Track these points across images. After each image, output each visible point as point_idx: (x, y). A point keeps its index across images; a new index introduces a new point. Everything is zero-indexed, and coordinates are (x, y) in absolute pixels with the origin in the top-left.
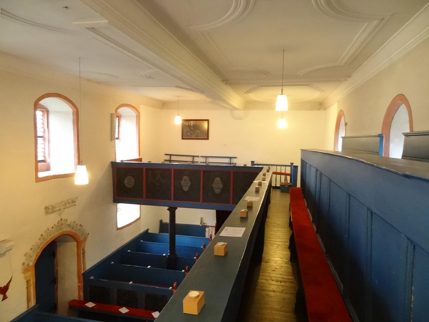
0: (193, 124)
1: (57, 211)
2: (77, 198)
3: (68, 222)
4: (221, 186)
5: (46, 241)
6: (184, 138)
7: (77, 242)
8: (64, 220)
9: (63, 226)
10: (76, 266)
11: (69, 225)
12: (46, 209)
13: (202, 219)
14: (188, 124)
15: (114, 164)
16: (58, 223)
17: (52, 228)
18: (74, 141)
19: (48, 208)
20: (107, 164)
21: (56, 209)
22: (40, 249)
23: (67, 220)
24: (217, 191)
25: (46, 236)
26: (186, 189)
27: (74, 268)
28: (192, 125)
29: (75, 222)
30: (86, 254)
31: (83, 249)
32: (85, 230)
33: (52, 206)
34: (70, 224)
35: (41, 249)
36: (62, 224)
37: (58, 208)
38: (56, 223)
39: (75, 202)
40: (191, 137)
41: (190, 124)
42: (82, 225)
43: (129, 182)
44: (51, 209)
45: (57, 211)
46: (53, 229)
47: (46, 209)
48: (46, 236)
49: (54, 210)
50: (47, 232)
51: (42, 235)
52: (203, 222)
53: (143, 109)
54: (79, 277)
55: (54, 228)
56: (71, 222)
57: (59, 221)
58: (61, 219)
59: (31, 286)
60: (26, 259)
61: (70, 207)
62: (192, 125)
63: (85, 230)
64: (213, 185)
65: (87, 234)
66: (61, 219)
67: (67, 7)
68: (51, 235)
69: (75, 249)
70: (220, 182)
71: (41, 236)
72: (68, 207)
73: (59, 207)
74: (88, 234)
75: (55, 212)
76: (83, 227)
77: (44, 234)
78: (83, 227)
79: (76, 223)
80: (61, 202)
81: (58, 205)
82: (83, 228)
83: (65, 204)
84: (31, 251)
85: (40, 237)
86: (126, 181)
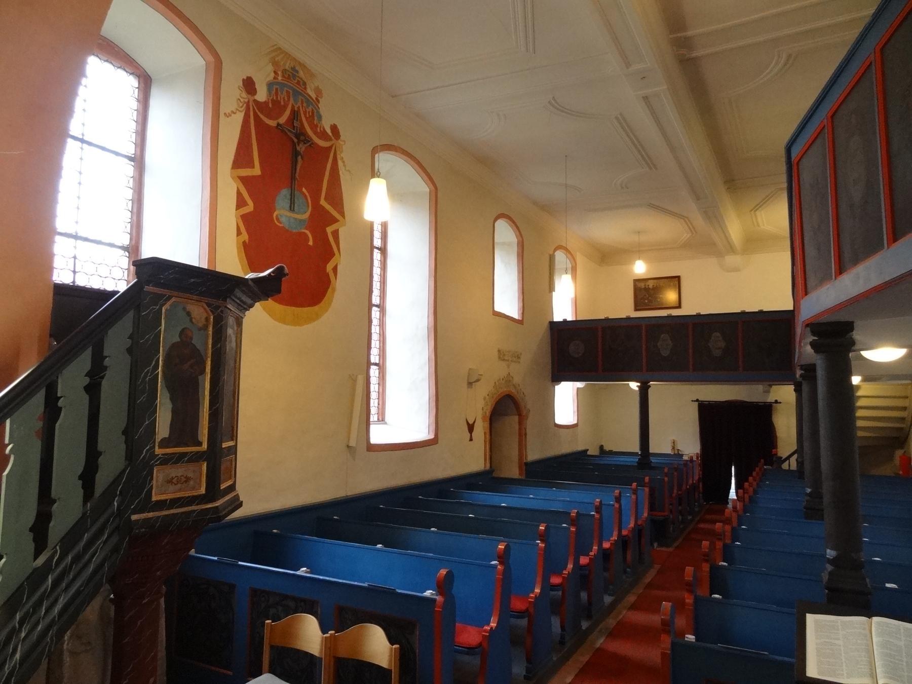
0: (653, 285)
4: (722, 344)
6: (637, 308)
7: (520, 415)
10: (517, 453)
11: (514, 385)
13: (674, 443)
14: (645, 285)
15: (553, 325)
18: (519, 280)
20: (546, 324)
24: (717, 353)
26: (665, 353)
27: (515, 453)
28: (651, 286)
30: (527, 437)
40: (650, 306)
41: (648, 286)
43: (576, 349)
52: (676, 448)
53: (580, 259)
54: (520, 468)
62: (651, 286)
64: (709, 344)
67: (644, 78)
69: (517, 427)
70: (721, 338)
86: (572, 348)
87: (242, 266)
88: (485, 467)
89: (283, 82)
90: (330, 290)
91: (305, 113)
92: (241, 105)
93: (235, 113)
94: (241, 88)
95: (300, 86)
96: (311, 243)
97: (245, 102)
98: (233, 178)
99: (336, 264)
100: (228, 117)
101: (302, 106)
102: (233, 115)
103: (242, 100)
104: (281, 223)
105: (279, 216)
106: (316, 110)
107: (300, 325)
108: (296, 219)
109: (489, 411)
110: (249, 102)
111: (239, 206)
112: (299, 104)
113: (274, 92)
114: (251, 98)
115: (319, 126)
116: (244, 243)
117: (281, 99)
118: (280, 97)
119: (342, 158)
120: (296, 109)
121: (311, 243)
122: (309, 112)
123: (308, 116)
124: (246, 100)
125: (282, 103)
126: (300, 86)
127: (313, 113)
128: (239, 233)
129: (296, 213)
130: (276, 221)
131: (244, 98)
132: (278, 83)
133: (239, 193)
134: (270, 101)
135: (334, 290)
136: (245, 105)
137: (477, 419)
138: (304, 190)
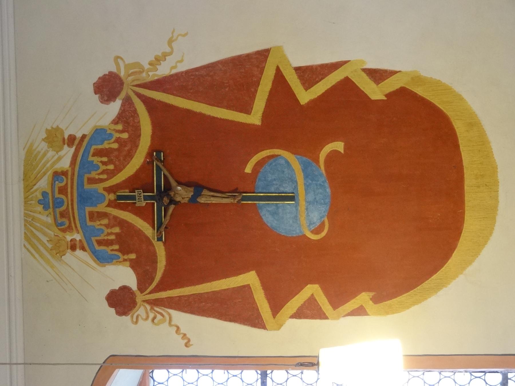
87: (415, 303)
89: (78, 225)
90: (419, 91)
91: (112, 174)
92: (159, 317)
93: (178, 328)
94: (135, 320)
95: (67, 184)
96: (339, 146)
97: (152, 309)
98: (279, 326)
99: (364, 75)
100: (189, 340)
101: (102, 181)
102: (182, 331)
103: (151, 315)
104: (323, 224)
105: (312, 227)
106: (89, 145)
107: (494, 169)
108: (307, 187)
110: (148, 302)
111: (321, 315)
112: (100, 187)
113: (108, 249)
114: (140, 297)
115: (117, 135)
116: (376, 300)
117: (111, 234)
118: (111, 234)
119: (151, 64)
120: (112, 197)
121: (339, 146)
122: (104, 163)
123: (111, 167)
124: (148, 307)
125: (117, 230)
126: (67, 184)
127: (99, 153)
128: (360, 311)
129: (296, 188)
130: (323, 234)
131: (147, 313)
132: (88, 233)
133: (299, 315)
134: (126, 257)
135: (418, 79)
136: (156, 308)
138: (248, 169)
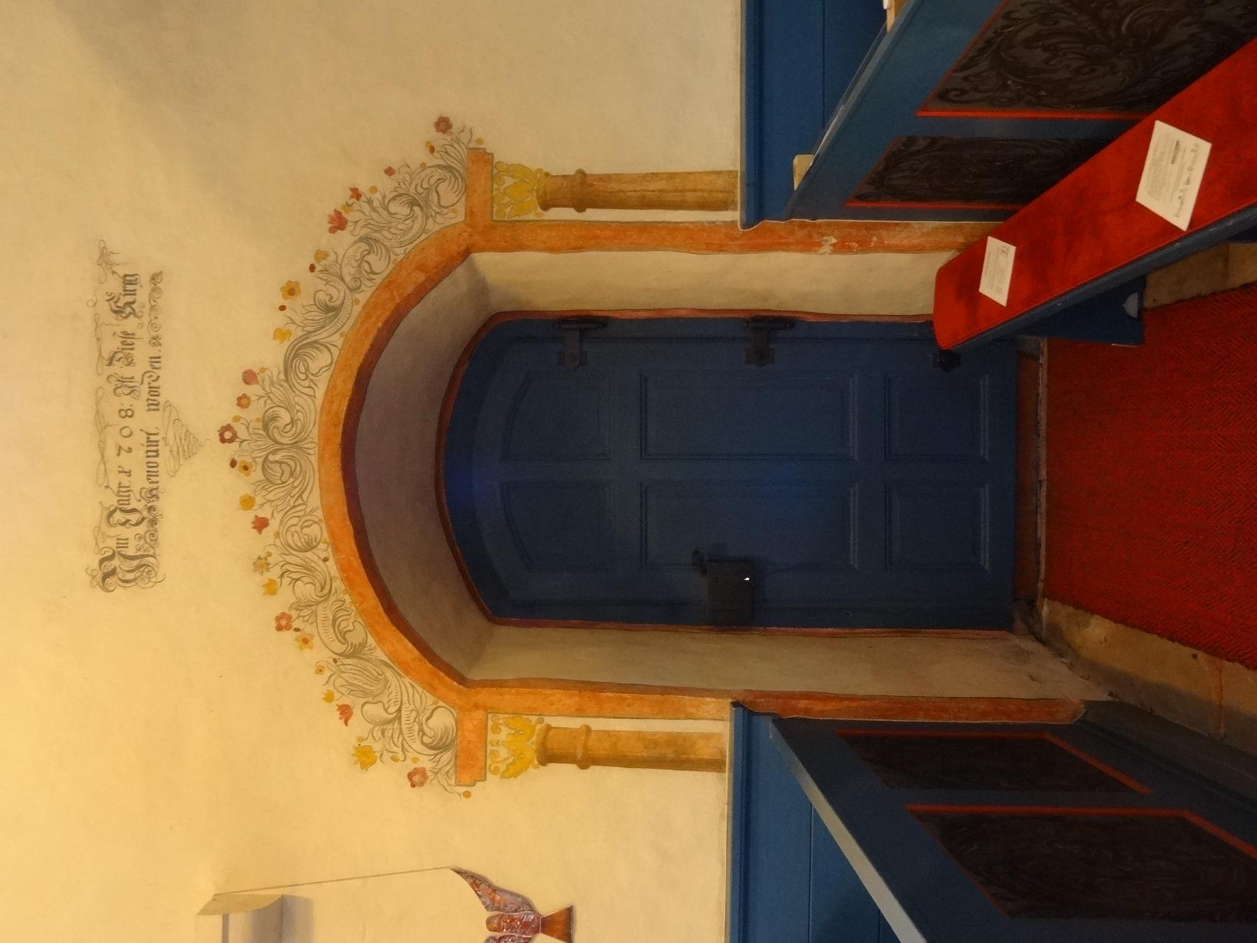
1: (152, 473)
2: (105, 259)
3: (271, 356)
5: (338, 585)
8: (243, 401)
9: (285, 417)
11: (295, 356)
12: (113, 573)
16: (246, 468)
17: (261, 524)
19: (112, 557)
21: (139, 481)
22: (371, 641)
23: (249, 377)
25: (306, 590)
29: (291, 290)
31: (546, 206)
32: (389, 171)
33: (111, 514)
34: (286, 344)
35: (376, 635)
36: (267, 423)
37: (136, 462)
38: (241, 485)
39: (129, 281)
42: (337, 199)
44: (128, 533)
45: (152, 473)
46: (274, 525)
47: (113, 573)
48: (306, 590)
49: (140, 506)
50: (275, 573)
51: (283, 623)
55: (265, 513)
56: (280, 334)
57: (233, 464)
58: (227, 435)
59: (588, 730)
60: (395, 759)
61: (155, 341)
63: (389, 171)
65: (440, 139)
66: (227, 435)
68: (310, 546)
71: (288, 627)
72: (155, 361)
73: (130, 450)
74: (443, 125)
75: (153, 494)
76: (356, 194)
77: (283, 601)
78: (364, 188)
79: (298, 271)
80: (101, 426)
81: (111, 451)
82: (374, 189)
83: (123, 383)
84: (356, 711)
85: (289, 635)
88: (713, 765)
109: (430, 699)
137: (466, 866)
